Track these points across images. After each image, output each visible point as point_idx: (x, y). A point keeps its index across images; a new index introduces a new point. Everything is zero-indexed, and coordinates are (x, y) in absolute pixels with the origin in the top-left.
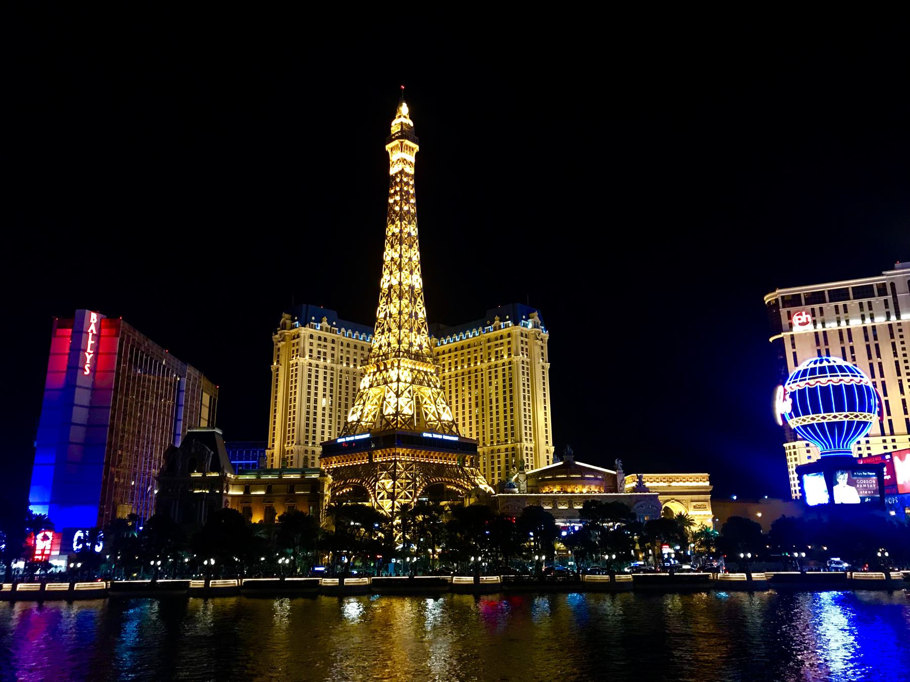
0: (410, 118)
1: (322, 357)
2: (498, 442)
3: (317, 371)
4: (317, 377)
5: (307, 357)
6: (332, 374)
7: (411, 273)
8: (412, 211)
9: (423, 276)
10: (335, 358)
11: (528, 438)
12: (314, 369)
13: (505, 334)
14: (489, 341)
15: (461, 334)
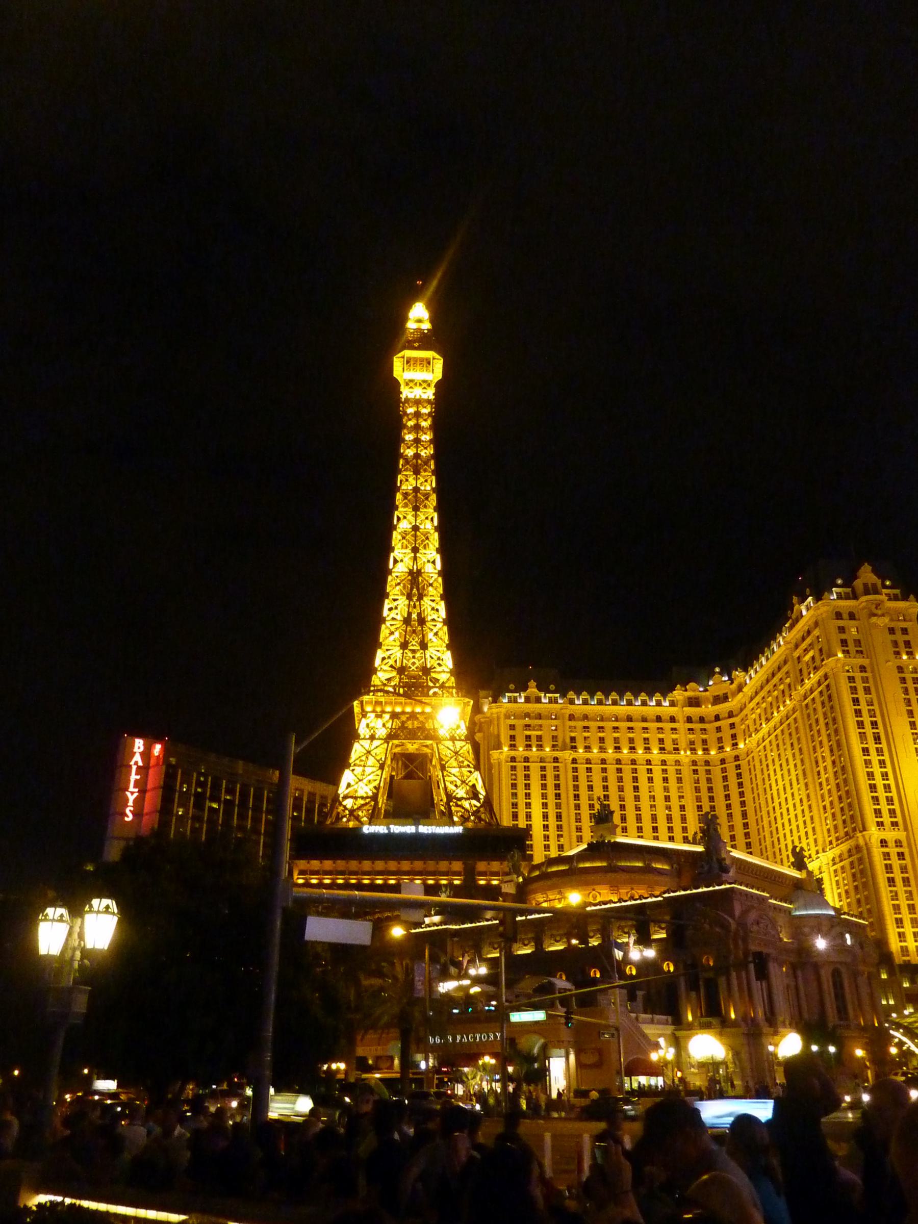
0: (432, 321)
1: (534, 742)
2: (837, 839)
3: (527, 768)
4: (527, 777)
5: (506, 749)
6: (556, 768)
7: (415, 550)
8: (424, 453)
9: (443, 550)
10: (560, 743)
11: (887, 819)
12: (520, 766)
13: (811, 622)
14: (797, 646)
15: (767, 653)
